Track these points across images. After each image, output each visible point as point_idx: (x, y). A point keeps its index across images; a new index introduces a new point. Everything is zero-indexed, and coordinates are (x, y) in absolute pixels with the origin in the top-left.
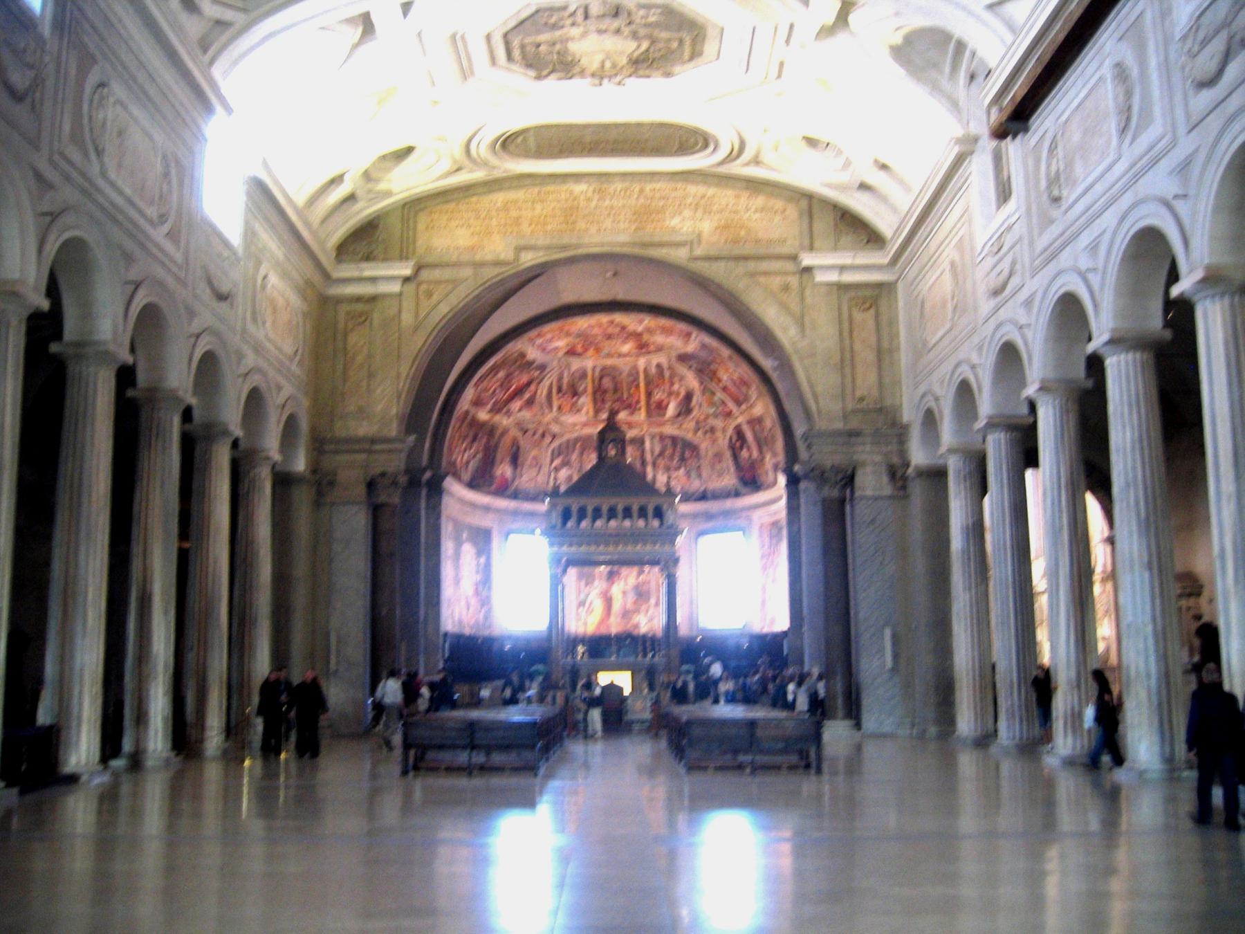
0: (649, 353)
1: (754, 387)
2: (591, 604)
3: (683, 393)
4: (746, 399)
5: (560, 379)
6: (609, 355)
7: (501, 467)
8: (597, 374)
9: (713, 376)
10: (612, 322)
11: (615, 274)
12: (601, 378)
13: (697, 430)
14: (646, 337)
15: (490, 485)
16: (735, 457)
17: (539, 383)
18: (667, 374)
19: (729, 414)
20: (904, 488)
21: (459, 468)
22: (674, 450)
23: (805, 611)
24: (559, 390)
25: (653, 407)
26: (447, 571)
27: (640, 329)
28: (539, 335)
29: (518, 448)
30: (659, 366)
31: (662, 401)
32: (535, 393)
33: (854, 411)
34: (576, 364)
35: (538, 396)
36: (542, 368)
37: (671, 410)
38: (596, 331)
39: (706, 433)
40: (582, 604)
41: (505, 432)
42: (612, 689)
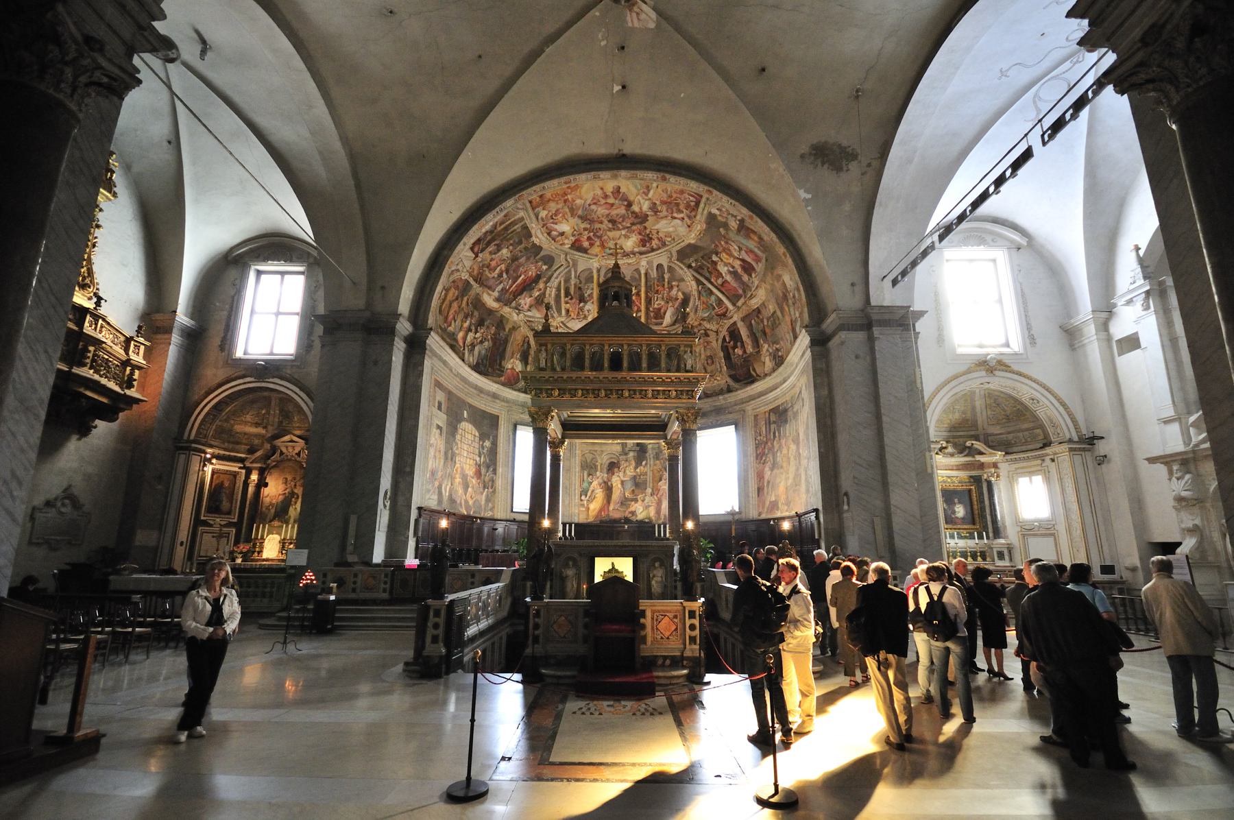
0: (653, 250)
1: (759, 267)
2: (593, 491)
3: (680, 296)
4: (746, 287)
5: (567, 280)
7: (512, 361)
10: (617, 191)
15: (500, 376)
16: (728, 357)
18: (666, 276)
19: (724, 315)
24: (567, 294)
25: (652, 314)
27: (646, 206)
28: (543, 202)
30: (660, 266)
31: (659, 309)
32: (544, 294)
35: (547, 296)
36: (549, 260)
38: (601, 211)
40: (584, 492)
41: (514, 328)
42: (614, 578)
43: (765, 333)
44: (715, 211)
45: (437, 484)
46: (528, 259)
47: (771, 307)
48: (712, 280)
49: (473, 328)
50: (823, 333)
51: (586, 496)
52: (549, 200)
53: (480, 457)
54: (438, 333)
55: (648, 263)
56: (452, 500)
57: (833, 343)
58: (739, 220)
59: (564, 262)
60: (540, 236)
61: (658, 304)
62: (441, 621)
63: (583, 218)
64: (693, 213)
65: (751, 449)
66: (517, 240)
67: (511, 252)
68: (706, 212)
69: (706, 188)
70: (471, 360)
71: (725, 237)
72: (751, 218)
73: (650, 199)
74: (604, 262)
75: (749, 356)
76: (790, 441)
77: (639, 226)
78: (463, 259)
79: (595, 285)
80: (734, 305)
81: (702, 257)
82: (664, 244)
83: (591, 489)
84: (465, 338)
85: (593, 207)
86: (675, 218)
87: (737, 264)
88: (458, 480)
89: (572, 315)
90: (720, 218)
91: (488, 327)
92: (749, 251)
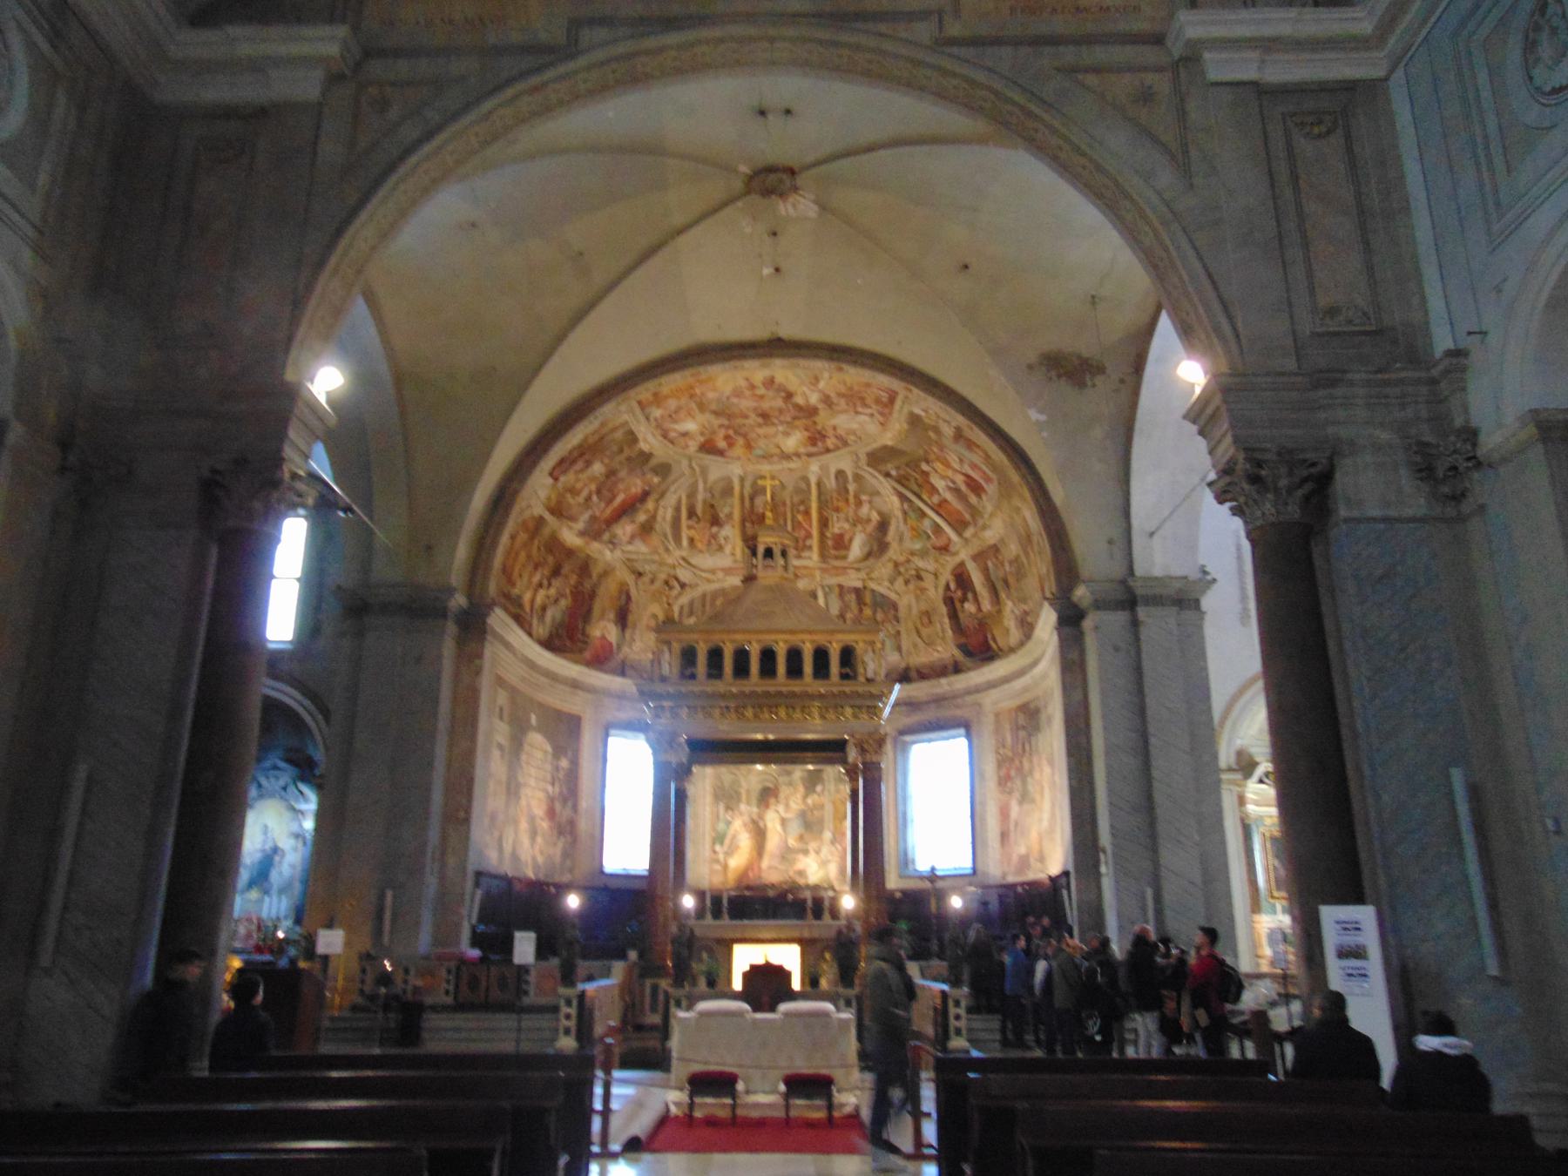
0: (828, 451)
1: (991, 489)
2: (734, 837)
3: (875, 517)
4: (975, 512)
5: (692, 495)
6: (767, 457)
8: (748, 490)
9: (926, 484)
10: (769, 383)
11: (777, 270)
12: (752, 499)
13: (892, 581)
14: (824, 420)
15: (581, 651)
16: (954, 616)
17: (662, 495)
18: (852, 487)
19: (945, 549)
20: (1458, 498)
21: (527, 608)
22: (861, 610)
23: (1105, 838)
24: (692, 513)
26: (491, 767)
27: (814, 399)
28: (658, 399)
29: (629, 598)
30: (840, 474)
31: (841, 536)
32: (654, 517)
33: (1315, 335)
34: (718, 469)
35: (659, 518)
36: (664, 470)
37: (856, 549)
38: (746, 404)
39: (907, 582)
41: (606, 573)
43: (1006, 582)
44: (917, 411)
45: (496, 834)
46: (631, 471)
47: (1013, 549)
48: (925, 497)
49: (545, 582)
50: (1075, 606)
51: (722, 843)
52: (666, 397)
53: (553, 784)
54: (506, 610)
55: (821, 468)
56: (515, 857)
57: (1087, 624)
58: (955, 428)
59: (687, 471)
60: (650, 438)
61: (839, 529)
62: (573, 1011)
63: (716, 413)
64: (886, 411)
65: (990, 768)
66: (615, 448)
67: (606, 465)
68: (905, 411)
69: (903, 384)
70: (541, 631)
71: (936, 442)
72: (972, 429)
73: (820, 391)
74: (750, 468)
75: (985, 617)
76: (1044, 762)
77: (804, 421)
78: (539, 489)
79: (736, 501)
80: (960, 534)
81: (907, 465)
82: (845, 444)
83: (731, 832)
84: (533, 601)
85: (735, 400)
86: (860, 413)
87: (960, 479)
88: (524, 825)
89: (699, 545)
90: (926, 421)
91: (566, 577)
92: (974, 466)
